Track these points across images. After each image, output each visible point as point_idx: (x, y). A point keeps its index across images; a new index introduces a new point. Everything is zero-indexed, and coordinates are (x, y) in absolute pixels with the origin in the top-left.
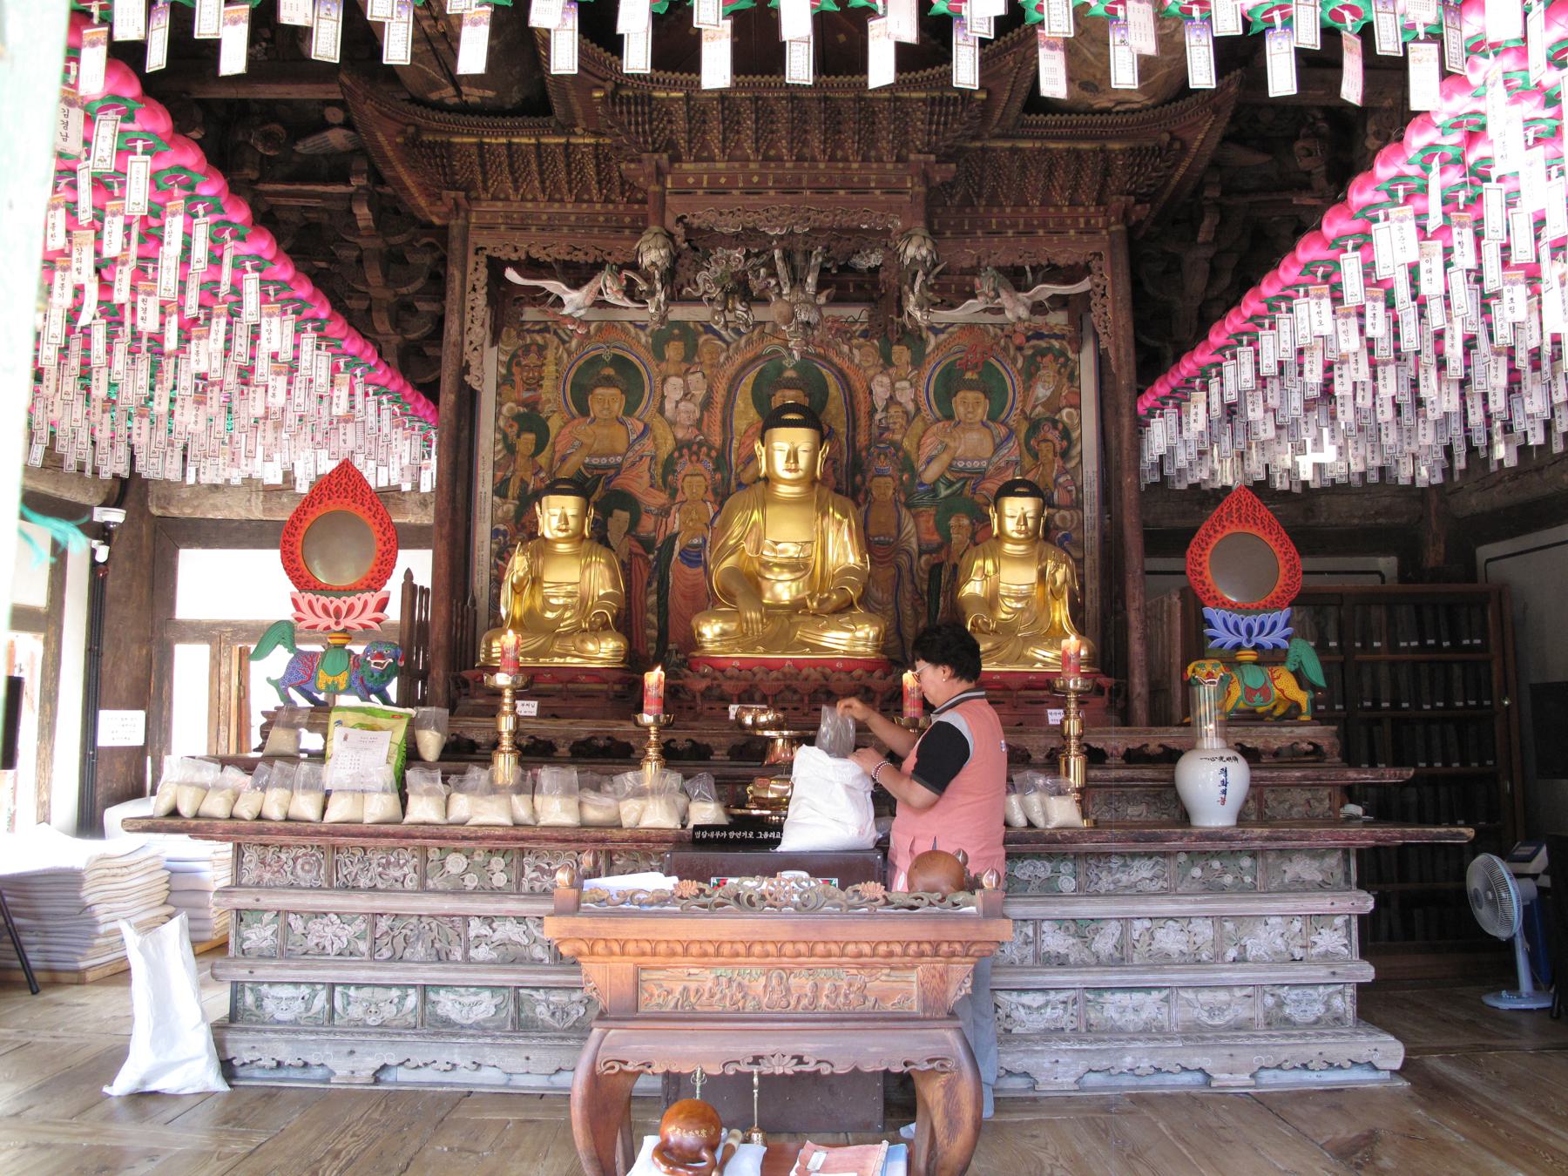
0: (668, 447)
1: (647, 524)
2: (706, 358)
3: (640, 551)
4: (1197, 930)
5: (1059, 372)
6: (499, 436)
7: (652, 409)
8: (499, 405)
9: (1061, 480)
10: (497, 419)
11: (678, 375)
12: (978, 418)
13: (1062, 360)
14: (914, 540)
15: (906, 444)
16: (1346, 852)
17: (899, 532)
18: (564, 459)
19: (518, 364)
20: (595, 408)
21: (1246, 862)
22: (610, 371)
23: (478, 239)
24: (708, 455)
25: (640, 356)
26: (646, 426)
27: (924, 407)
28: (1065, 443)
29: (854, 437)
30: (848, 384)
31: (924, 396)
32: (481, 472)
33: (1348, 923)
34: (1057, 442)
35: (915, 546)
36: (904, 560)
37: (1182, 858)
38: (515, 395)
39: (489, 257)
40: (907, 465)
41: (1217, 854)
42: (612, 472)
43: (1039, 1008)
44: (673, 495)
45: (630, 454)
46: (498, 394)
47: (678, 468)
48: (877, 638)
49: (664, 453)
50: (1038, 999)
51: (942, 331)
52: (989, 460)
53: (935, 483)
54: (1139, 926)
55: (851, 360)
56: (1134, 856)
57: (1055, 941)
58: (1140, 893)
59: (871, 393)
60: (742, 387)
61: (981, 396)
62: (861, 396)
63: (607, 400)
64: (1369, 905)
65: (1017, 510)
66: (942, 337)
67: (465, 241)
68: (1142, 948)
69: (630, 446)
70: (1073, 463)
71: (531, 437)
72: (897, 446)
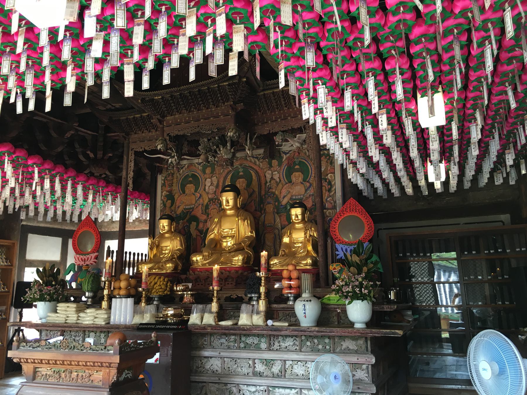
0: (206, 201)
1: (201, 226)
2: (217, 172)
3: (199, 234)
4: (309, 366)
5: (327, 162)
6: (162, 202)
7: (202, 189)
8: (162, 192)
9: (328, 199)
10: (161, 197)
11: (209, 178)
12: (300, 181)
13: (328, 157)
14: (279, 224)
15: (277, 193)
16: (366, 338)
17: (275, 222)
18: (178, 207)
19: (167, 179)
20: (187, 191)
21: (327, 341)
22: (191, 179)
23: (132, 146)
24: (218, 202)
25: (199, 173)
26: (200, 195)
27: (282, 180)
28: (329, 186)
29: (260, 192)
30: (259, 175)
31: (282, 176)
32: (157, 213)
33: (367, 367)
34: (326, 186)
35: (280, 226)
36: (276, 231)
37: (303, 338)
38: (166, 189)
39: (135, 151)
40: (277, 200)
41: (316, 337)
42: (191, 210)
43: (254, 392)
44: (208, 216)
45: (196, 204)
46: (162, 189)
47: (209, 207)
48: (243, 259)
49: (205, 203)
50: (253, 389)
51: (288, 153)
52: (303, 195)
53: (286, 205)
54: (288, 363)
55: (259, 167)
56: (287, 336)
57: (260, 367)
58: (289, 351)
59: (265, 177)
60: (227, 180)
61: (301, 173)
62: (263, 178)
63: (190, 188)
64: (374, 361)
65: (296, 212)
66: (288, 155)
67: (129, 147)
68: (289, 372)
69: (196, 201)
70: (332, 193)
71: (170, 201)
72: (274, 193)
